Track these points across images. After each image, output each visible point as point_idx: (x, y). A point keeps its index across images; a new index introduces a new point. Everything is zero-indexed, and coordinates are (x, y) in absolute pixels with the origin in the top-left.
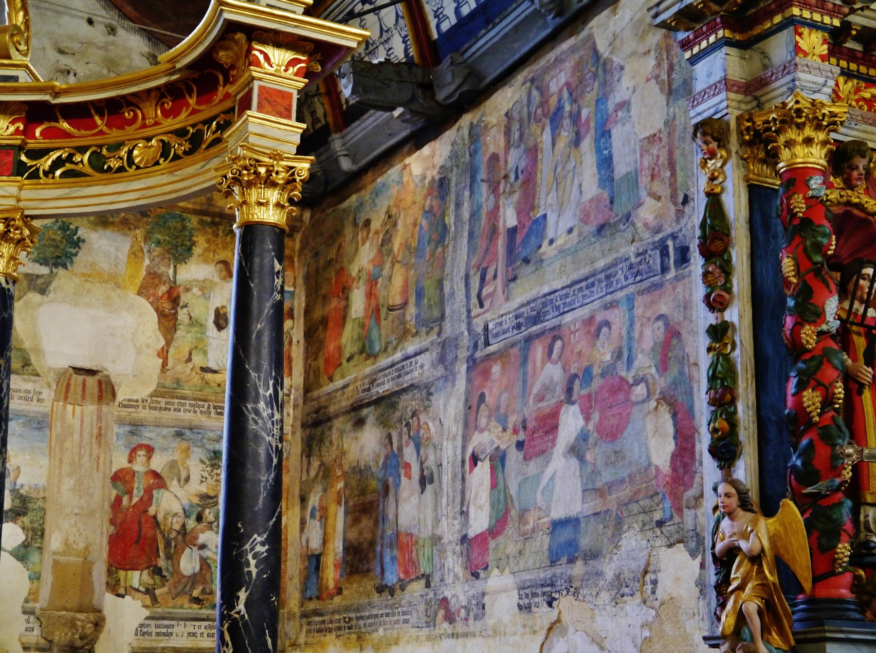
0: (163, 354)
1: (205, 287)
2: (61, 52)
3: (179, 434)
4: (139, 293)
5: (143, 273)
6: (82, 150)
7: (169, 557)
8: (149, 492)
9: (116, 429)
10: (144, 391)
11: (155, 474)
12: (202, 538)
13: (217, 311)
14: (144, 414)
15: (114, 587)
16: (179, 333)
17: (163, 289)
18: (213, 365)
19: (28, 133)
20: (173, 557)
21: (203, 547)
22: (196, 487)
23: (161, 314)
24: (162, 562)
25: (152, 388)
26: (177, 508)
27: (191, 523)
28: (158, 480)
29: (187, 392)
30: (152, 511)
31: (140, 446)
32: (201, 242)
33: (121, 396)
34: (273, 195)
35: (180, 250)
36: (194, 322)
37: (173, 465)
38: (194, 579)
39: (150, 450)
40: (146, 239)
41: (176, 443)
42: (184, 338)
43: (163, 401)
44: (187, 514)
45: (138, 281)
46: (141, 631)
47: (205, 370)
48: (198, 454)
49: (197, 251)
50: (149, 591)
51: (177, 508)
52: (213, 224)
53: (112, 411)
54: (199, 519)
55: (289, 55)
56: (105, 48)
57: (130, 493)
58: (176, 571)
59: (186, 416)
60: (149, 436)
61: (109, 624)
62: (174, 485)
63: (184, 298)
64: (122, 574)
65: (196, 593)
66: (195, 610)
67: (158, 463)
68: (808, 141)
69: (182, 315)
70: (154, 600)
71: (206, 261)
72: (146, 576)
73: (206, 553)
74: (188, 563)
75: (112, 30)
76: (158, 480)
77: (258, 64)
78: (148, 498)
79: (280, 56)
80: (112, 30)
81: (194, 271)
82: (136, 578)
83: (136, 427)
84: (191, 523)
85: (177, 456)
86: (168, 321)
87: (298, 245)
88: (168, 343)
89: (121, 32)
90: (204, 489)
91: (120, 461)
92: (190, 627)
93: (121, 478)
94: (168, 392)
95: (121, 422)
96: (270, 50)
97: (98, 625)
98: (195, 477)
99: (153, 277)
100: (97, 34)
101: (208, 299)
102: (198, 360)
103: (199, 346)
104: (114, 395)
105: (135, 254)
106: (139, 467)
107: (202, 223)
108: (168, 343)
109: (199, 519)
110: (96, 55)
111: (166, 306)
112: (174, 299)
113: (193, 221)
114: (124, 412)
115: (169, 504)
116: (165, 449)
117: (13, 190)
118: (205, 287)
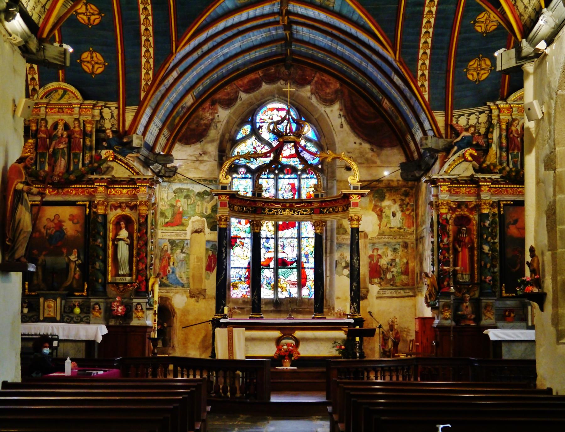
0: (379, 225)
1: (389, 207)
2: (349, 153)
3: (385, 245)
4: (372, 211)
5: (373, 205)
6: (331, 207)
7: (384, 275)
8: (378, 259)
9: (369, 245)
10: (375, 235)
11: (379, 255)
12: (392, 270)
13: (393, 213)
14: (376, 241)
15: (371, 282)
16: (384, 219)
17: (378, 209)
18: (392, 226)
19: (321, 205)
20: (385, 274)
21: (392, 272)
22: (390, 257)
23: (378, 215)
24: (382, 276)
25: (377, 234)
26: (385, 263)
27: (389, 266)
28: (380, 256)
29: (386, 234)
30: (379, 264)
31: (375, 249)
32: (387, 195)
33: (370, 237)
34: (355, 222)
35: (382, 198)
36: (387, 216)
37: (384, 252)
38: (391, 280)
39: (378, 249)
40: (373, 196)
41: (384, 247)
42: (385, 220)
43: (380, 237)
44: (388, 264)
45: (372, 208)
46: (378, 293)
47: (391, 228)
48: (390, 249)
49: (386, 197)
50: (380, 283)
51: (385, 263)
52: (391, 190)
53: (368, 240)
54: (391, 265)
55: (356, 196)
56: (359, 149)
57: (373, 260)
58: (386, 278)
59: (386, 240)
60: (377, 246)
61: (370, 291)
62: (384, 257)
63: (384, 210)
64: (373, 279)
65: (391, 283)
66: (391, 287)
67: (380, 252)
68: (443, 208)
69: (384, 215)
70: (381, 285)
71: (389, 200)
72: (379, 280)
73: (394, 273)
74: (389, 276)
75: (361, 144)
76: (380, 256)
77: (351, 198)
78: (378, 261)
79: (355, 196)
80: (361, 144)
81: (386, 203)
82: (376, 280)
83: (374, 244)
84: (389, 266)
85: (384, 250)
86: (380, 217)
87: (414, 192)
88: (381, 222)
89: (363, 144)
90: (392, 258)
91: (370, 253)
92: (390, 291)
93: (371, 257)
94: (381, 234)
95: (370, 243)
96: (354, 195)
97: (368, 291)
98: (389, 255)
99: (376, 206)
100: (357, 146)
101: (390, 209)
102: (388, 226)
103: (389, 222)
104: (368, 237)
105: (371, 201)
106: (375, 254)
107: (387, 190)
108: (381, 222)
109: (391, 265)
110: (357, 151)
111: (379, 213)
112: (381, 211)
113: (385, 190)
114: (370, 241)
115: (383, 262)
116: (381, 249)
117: (320, 216)
118: (389, 207)
